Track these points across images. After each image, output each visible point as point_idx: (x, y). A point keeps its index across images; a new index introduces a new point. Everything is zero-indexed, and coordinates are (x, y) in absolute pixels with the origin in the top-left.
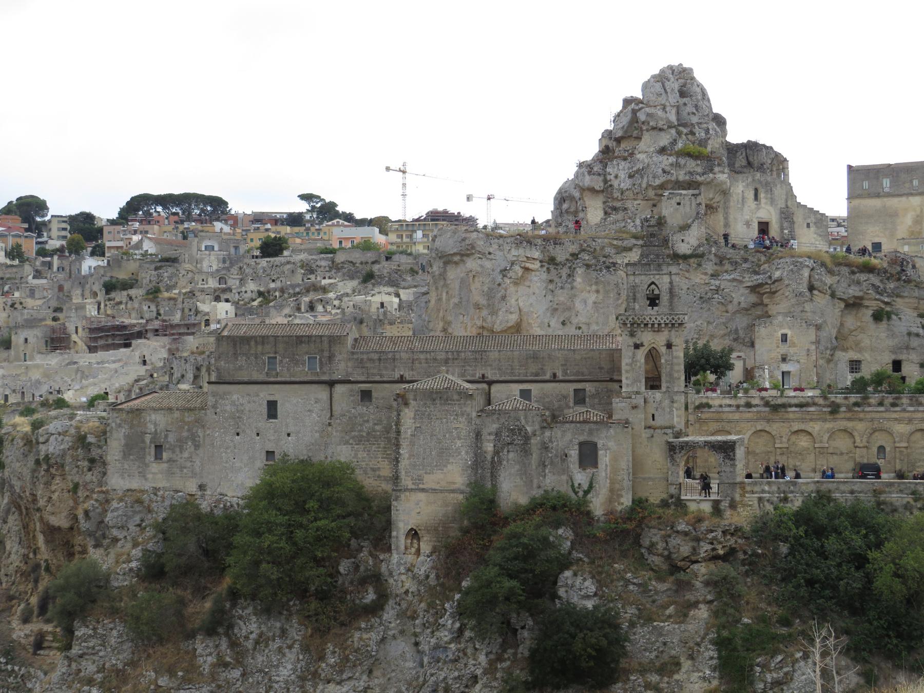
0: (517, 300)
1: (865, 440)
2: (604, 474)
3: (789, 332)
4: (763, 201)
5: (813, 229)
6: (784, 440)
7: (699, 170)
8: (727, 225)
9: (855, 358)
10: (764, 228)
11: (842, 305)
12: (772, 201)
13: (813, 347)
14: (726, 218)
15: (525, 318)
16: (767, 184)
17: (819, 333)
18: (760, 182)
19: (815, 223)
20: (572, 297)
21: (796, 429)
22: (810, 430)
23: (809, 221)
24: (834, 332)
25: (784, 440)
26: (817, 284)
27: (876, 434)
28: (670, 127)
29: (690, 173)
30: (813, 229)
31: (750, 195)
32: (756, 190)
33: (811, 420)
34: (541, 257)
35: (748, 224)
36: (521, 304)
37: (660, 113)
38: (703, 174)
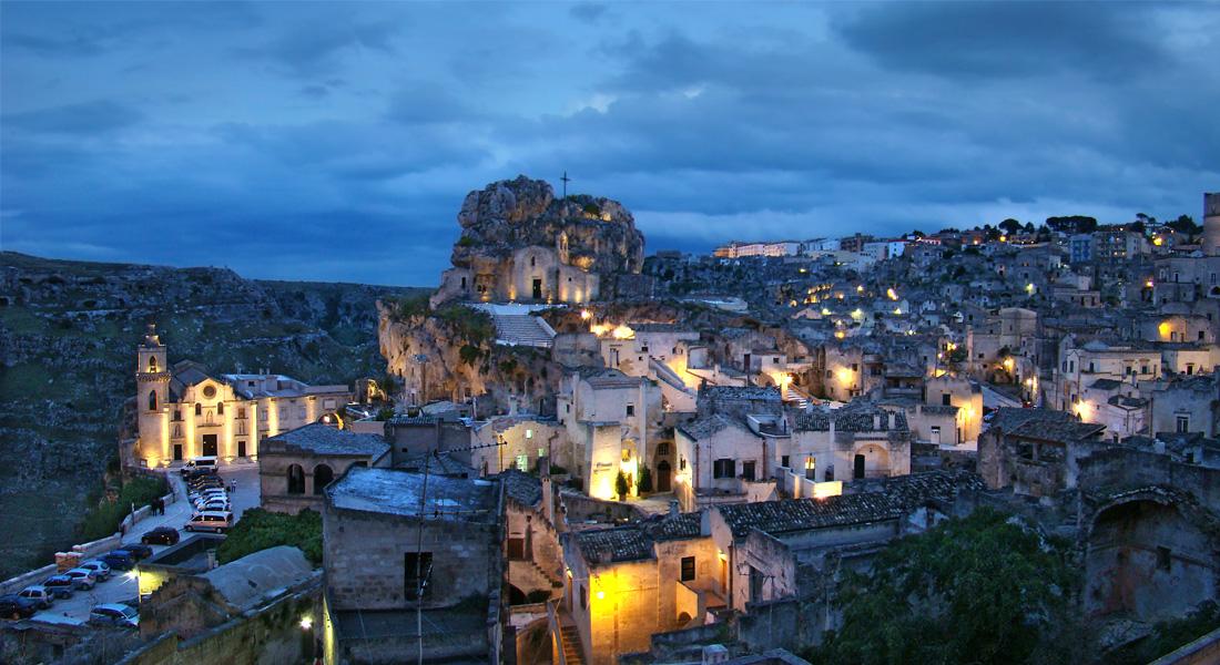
10: (537, 283)
31: (528, 261)
32: (533, 260)
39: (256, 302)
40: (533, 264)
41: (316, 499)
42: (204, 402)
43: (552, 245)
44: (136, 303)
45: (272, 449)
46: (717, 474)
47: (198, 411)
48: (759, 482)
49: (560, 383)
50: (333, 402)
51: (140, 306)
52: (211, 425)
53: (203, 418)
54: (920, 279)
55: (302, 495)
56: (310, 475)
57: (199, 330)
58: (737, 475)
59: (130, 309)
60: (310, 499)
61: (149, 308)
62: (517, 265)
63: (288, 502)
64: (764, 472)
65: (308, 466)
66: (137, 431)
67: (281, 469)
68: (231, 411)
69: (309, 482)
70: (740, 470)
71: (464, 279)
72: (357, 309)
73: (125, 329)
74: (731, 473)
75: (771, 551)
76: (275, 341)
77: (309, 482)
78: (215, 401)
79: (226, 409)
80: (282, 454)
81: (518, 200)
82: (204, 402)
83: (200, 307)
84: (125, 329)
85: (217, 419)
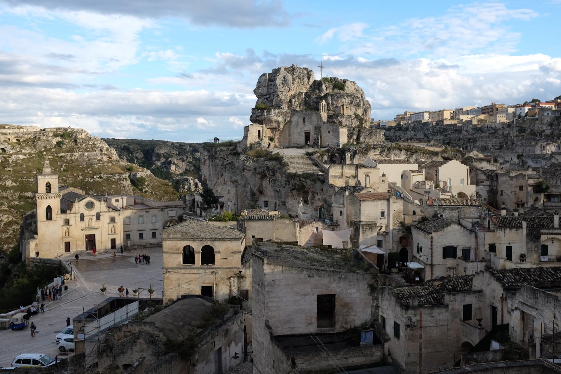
3: (229, 188)
4: (306, 123)
5: (331, 133)
7: (260, 114)
8: (290, 135)
9: (266, 200)
10: (307, 136)
11: (259, 176)
12: (311, 122)
14: (289, 133)
16: (309, 115)
18: (305, 114)
19: (333, 131)
23: (329, 130)
24: (255, 189)
26: (245, 167)
28: (262, 96)
30: (331, 133)
31: (301, 120)
35: (299, 134)
39: (101, 150)
40: (304, 122)
41: (203, 268)
42: (86, 213)
43: (317, 109)
44: (14, 151)
45: (171, 236)
46: (445, 256)
47: (82, 218)
48: (472, 262)
49: (333, 197)
51: (17, 153)
54: (544, 131)
55: (192, 266)
56: (199, 252)
57: (62, 169)
58: (457, 257)
59: (11, 155)
60: (199, 268)
61: (25, 154)
62: (293, 124)
63: (183, 271)
64: (476, 255)
65: (197, 247)
66: (36, 233)
67: (178, 249)
68: (106, 218)
69: (198, 258)
70: (459, 253)
71: (259, 131)
72: (165, 157)
73: (8, 169)
74: (454, 256)
75: (541, 300)
76: (117, 177)
77: (198, 258)
78: (94, 212)
79: (101, 217)
80: (180, 239)
81: (294, 80)
82: (86, 213)
83: (62, 154)
84: (8, 169)
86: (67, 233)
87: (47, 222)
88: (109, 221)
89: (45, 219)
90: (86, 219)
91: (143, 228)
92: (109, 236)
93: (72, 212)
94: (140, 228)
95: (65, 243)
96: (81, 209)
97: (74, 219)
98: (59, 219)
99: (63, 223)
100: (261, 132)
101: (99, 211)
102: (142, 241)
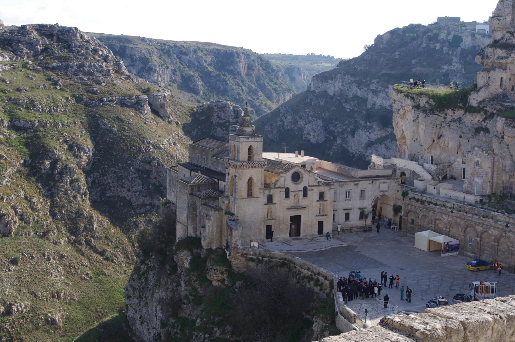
0: (402, 126)
1: (463, 231)
2: (208, 231)
3: (479, 159)
6: (433, 223)
13: (490, 170)
15: (405, 134)
17: (504, 162)
20: (418, 127)
21: (437, 217)
22: (443, 219)
25: (433, 223)
27: (468, 229)
29: (498, 58)
33: (444, 214)
34: (413, 105)
36: (403, 128)
37: (496, 21)
38: (505, 58)
42: (292, 186)
50: (386, 185)
52: (297, 208)
53: (290, 202)
79: (309, 193)
82: (292, 186)
85: (303, 202)
86: (269, 213)
87: (248, 199)
88: (318, 198)
89: (246, 197)
90: (291, 195)
91: (349, 207)
92: (317, 218)
93: (277, 186)
94: (346, 207)
95: (267, 226)
96: (286, 182)
97: (278, 196)
98: (261, 195)
99: (266, 201)
100: (504, 79)
101: (307, 185)
102: (347, 222)
